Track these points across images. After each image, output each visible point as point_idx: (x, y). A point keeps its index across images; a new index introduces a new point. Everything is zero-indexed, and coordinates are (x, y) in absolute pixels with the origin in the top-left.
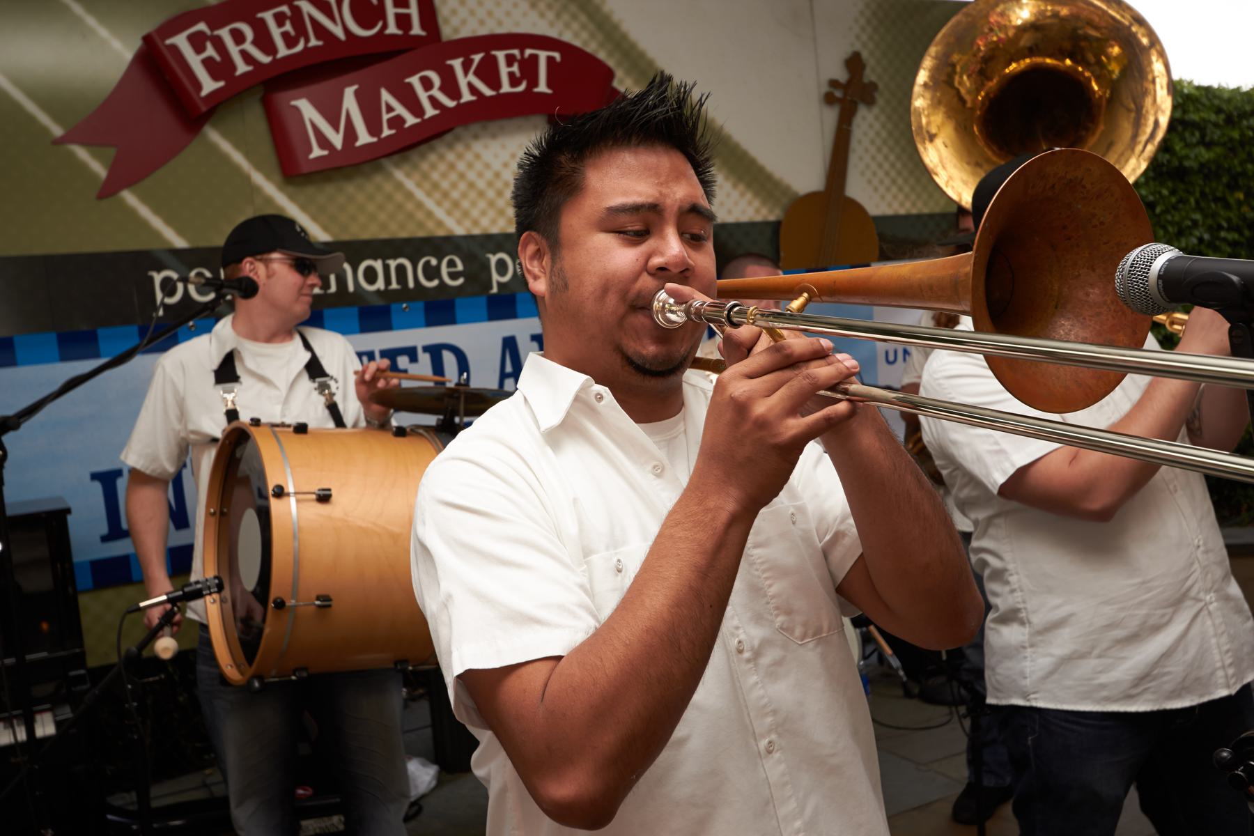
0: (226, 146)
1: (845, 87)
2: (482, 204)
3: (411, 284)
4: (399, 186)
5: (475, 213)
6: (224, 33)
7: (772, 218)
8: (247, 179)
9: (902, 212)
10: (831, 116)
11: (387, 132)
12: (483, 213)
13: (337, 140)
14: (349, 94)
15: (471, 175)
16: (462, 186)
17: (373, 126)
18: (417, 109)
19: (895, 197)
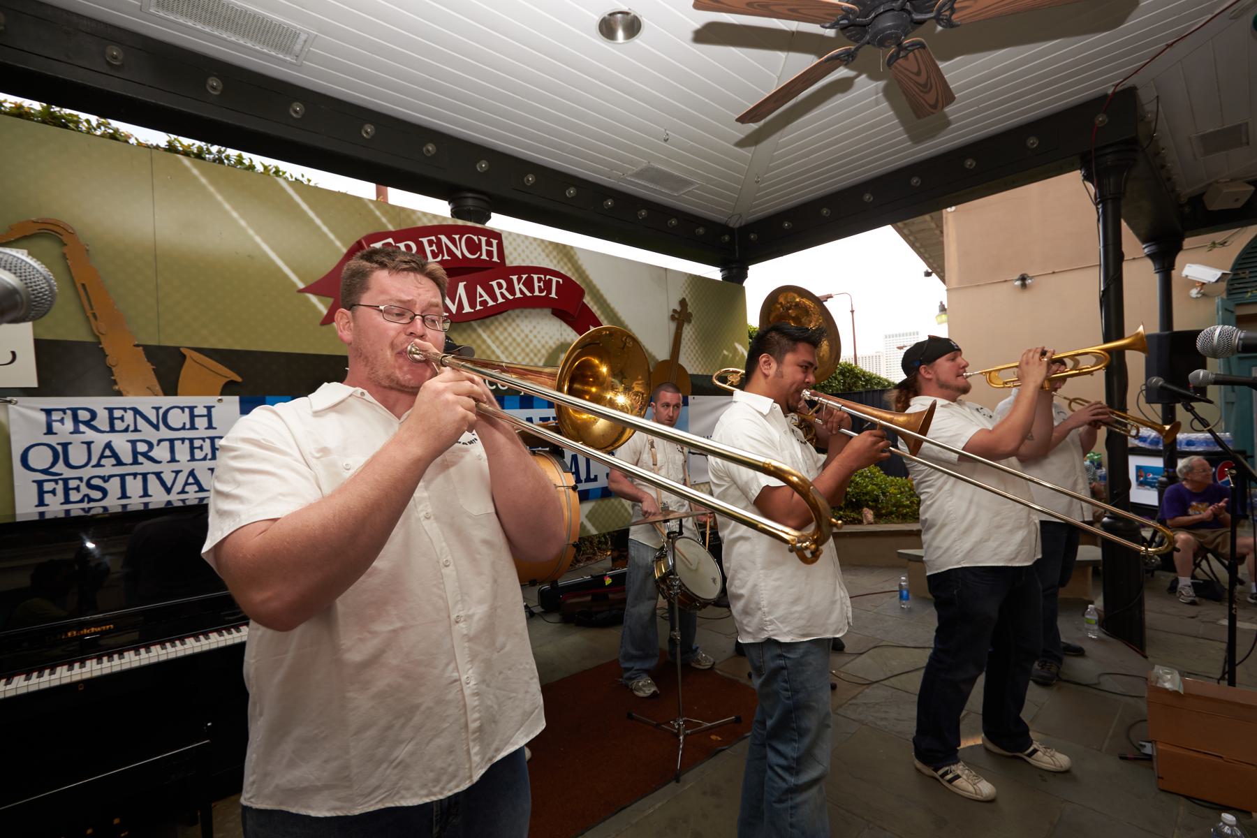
2: (519, 350)
4: (480, 336)
5: (515, 354)
9: (700, 373)
10: (673, 326)
11: (478, 308)
12: (519, 354)
13: (454, 309)
14: (461, 285)
15: (514, 335)
16: (510, 339)
17: (472, 304)
18: (494, 298)
19: (697, 366)
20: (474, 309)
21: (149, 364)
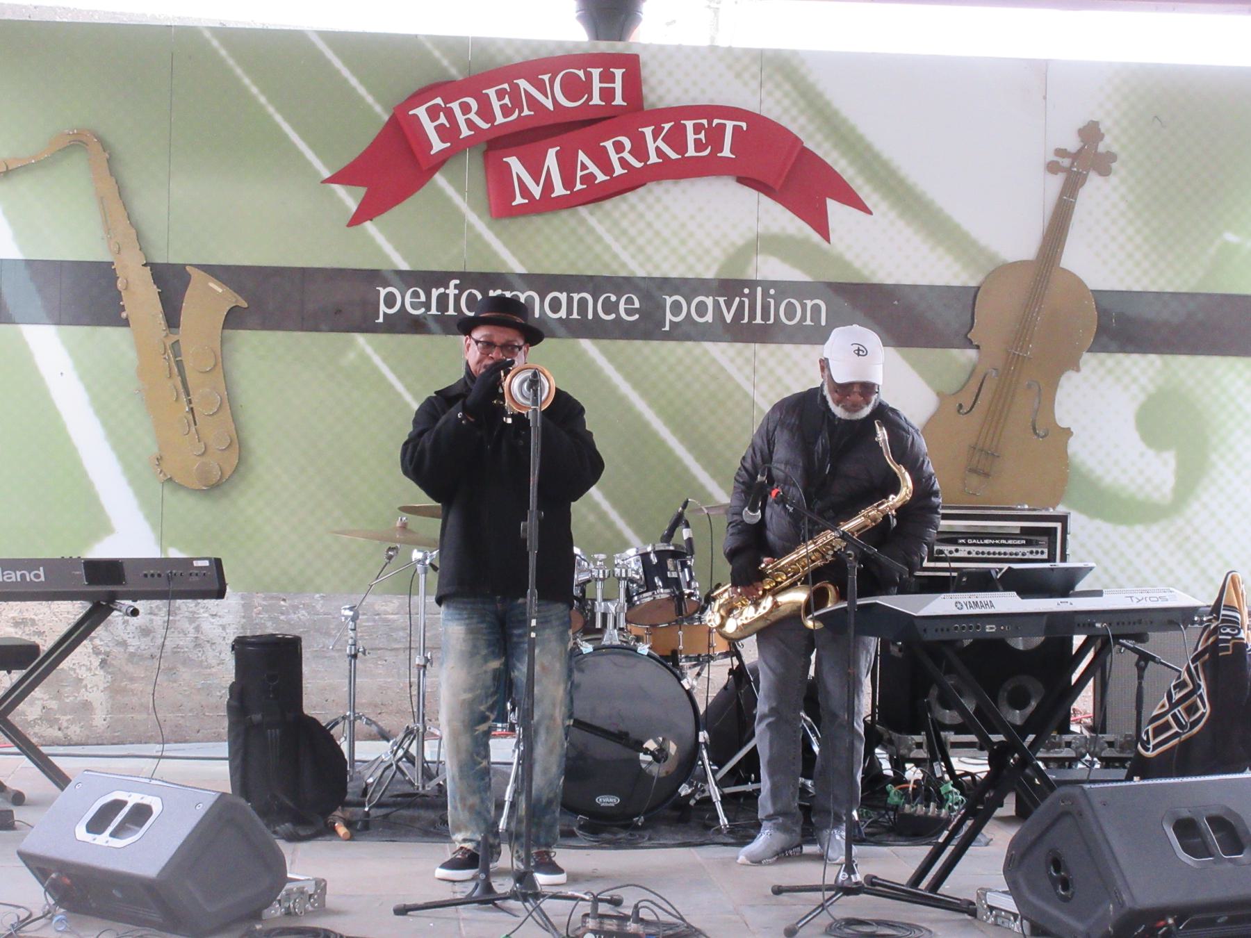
0: (450, 191)
1: (1075, 156)
3: (590, 316)
6: (455, 106)
7: (973, 283)
8: (462, 217)
9: (1137, 288)
11: (579, 187)
13: (536, 191)
14: (552, 154)
17: (568, 182)
18: (606, 167)
20: (572, 190)
21: (155, 287)
